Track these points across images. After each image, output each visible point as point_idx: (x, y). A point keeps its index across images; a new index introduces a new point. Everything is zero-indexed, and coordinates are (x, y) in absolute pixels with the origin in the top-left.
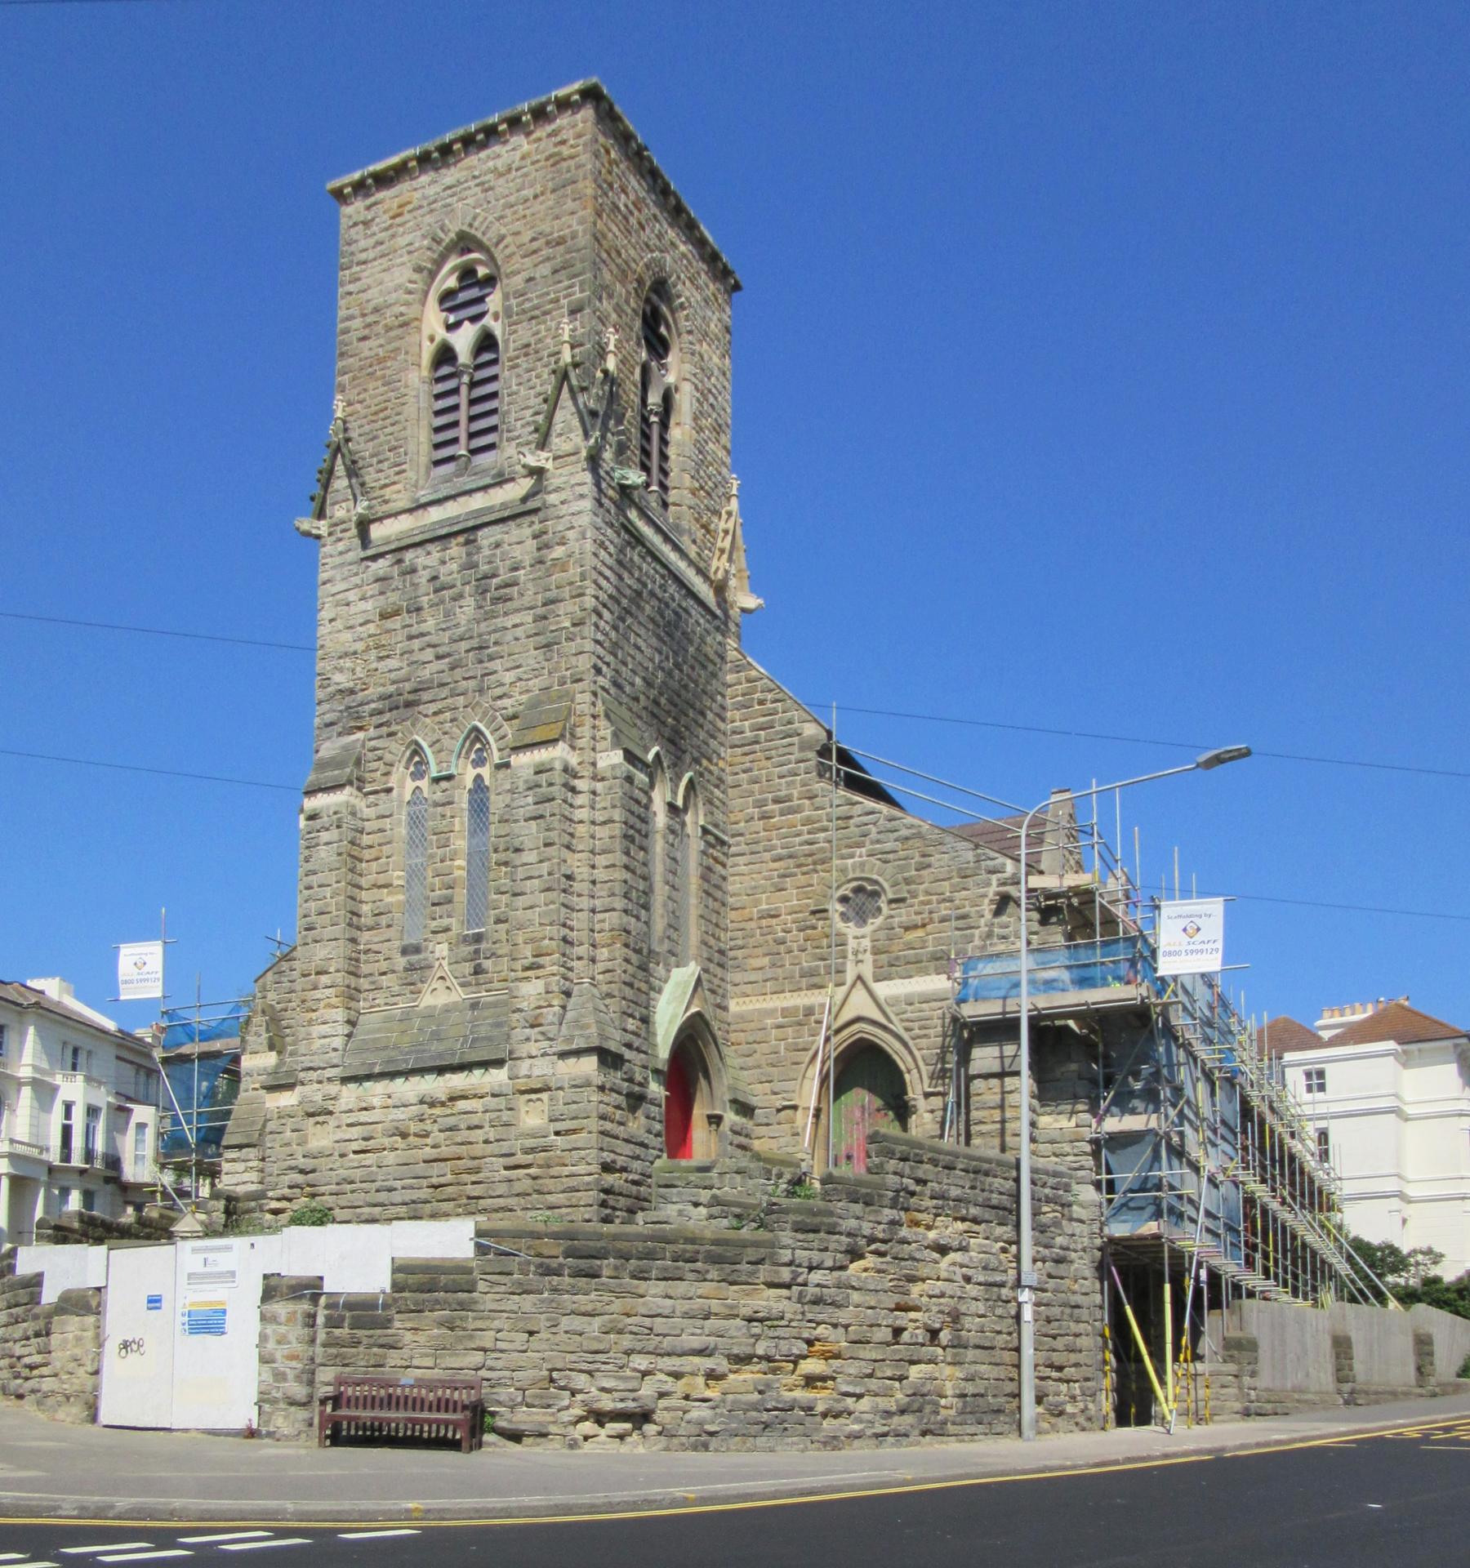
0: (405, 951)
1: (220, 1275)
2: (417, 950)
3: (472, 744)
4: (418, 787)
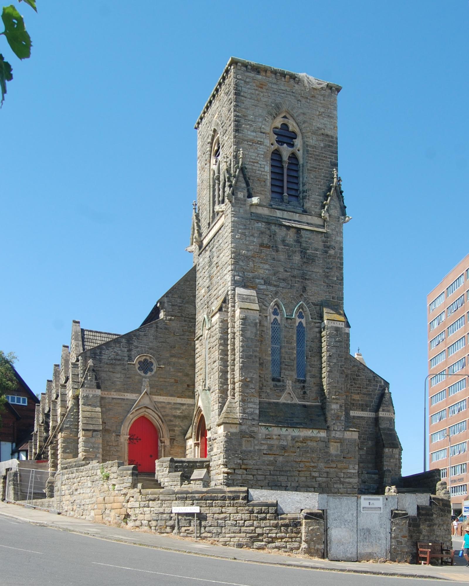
0: (273, 380)
1: (375, 508)
2: (279, 381)
3: (299, 309)
4: (275, 318)
